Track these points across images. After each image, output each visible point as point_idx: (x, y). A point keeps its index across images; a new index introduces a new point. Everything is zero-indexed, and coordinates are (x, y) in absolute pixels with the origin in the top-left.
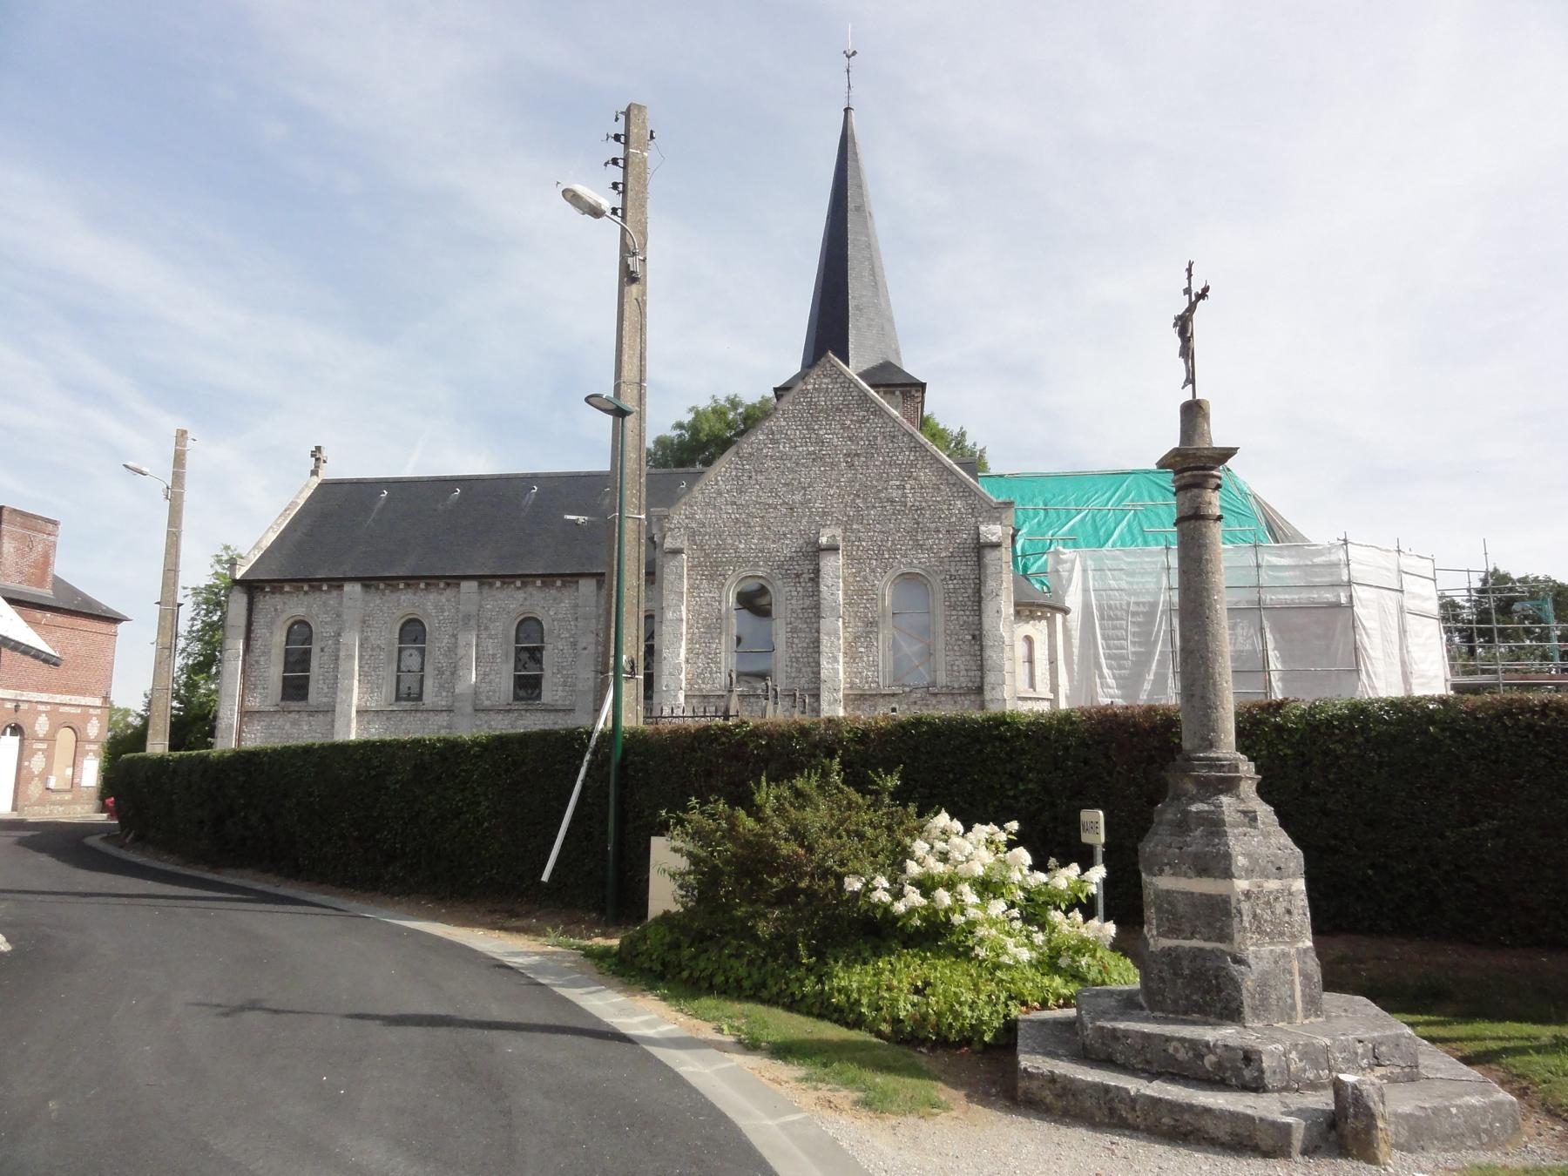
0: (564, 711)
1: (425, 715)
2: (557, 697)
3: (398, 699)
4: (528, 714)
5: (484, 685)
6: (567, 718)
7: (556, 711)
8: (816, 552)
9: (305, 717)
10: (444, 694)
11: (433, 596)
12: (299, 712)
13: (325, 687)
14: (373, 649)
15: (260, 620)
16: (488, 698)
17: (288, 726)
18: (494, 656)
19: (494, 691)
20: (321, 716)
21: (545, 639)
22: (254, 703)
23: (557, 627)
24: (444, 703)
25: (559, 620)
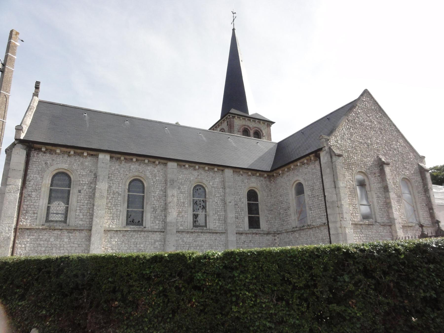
0: (220, 233)
1: (146, 233)
2: (216, 226)
3: (127, 224)
4: (202, 235)
5: (179, 218)
6: (221, 237)
7: (216, 233)
8: (381, 165)
9: (66, 233)
10: (157, 222)
11: (150, 168)
12: (61, 230)
13: (81, 214)
14: (114, 194)
15: (33, 168)
16: (181, 225)
17: (52, 240)
18: (184, 203)
19: (185, 222)
20: (77, 234)
21: (207, 196)
22: (25, 223)
23: (214, 191)
24: (157, 227)
25: (214, 188)
